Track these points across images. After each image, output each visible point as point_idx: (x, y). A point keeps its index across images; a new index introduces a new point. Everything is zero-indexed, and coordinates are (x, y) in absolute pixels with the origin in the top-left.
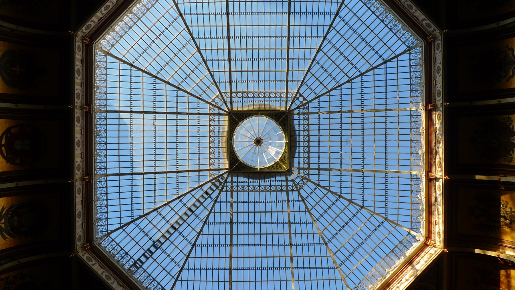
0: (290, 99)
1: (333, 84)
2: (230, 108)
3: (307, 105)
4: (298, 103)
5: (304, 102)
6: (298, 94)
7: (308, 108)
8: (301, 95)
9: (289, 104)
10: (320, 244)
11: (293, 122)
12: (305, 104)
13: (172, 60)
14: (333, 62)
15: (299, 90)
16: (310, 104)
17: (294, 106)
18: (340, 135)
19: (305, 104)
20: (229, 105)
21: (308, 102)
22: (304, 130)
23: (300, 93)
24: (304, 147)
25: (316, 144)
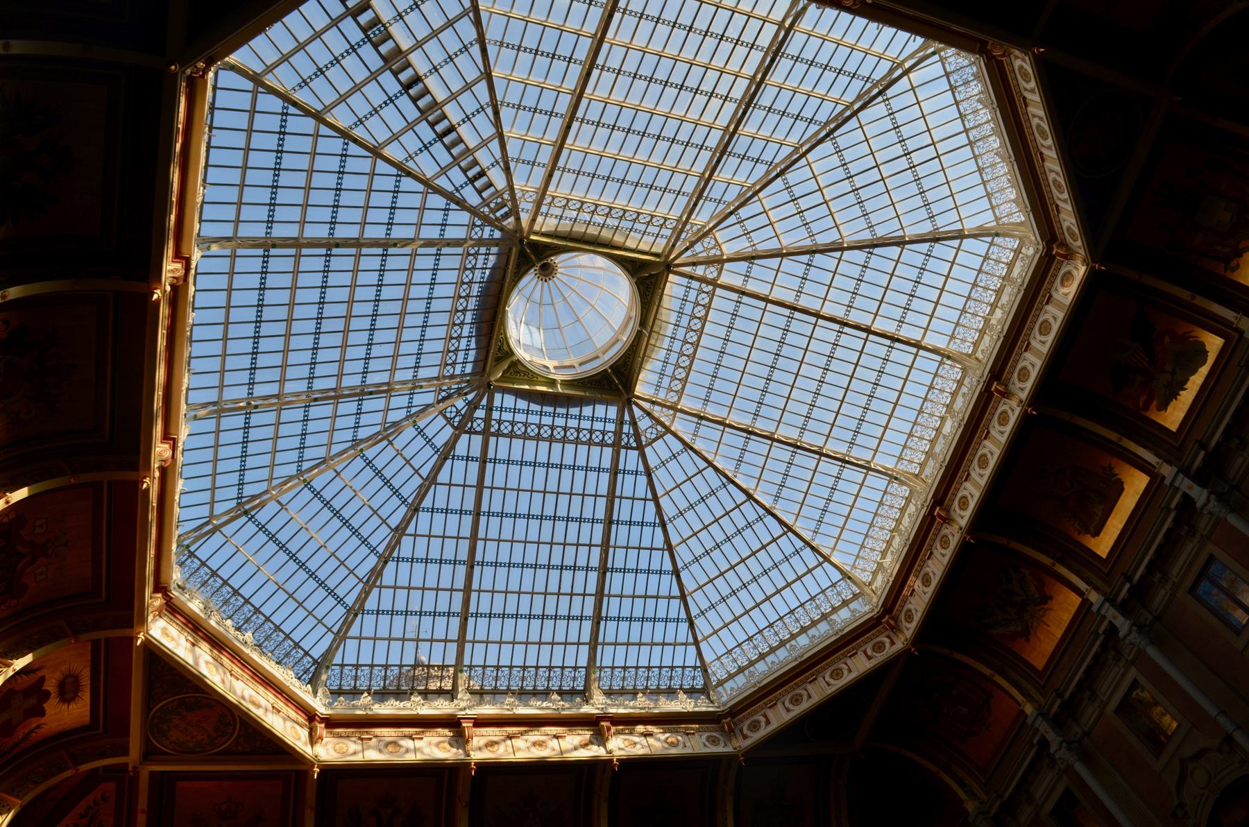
0: (657, 411)
1: (669, 509)
2: (677, 262)
3: (634, 445)
4: (644, 423)
5: (643, 438)
6: (663, 430)
7: (628, 447)
8: (661, 437)
9: (646, 405)
10: (301, 460)
11: (601, 402)
12: (638, 440)
13: (848, 178)
14: (689, 479)
15: (675, 435)
16: (636, 453)
17: (637, 412)
18: (555, 517)
19: (638, 440)
20: (688, 269)
21: (640, 448)
22: (578, 430)
23: (665, 434)
24: (540, 426)
25: (542, 458)
